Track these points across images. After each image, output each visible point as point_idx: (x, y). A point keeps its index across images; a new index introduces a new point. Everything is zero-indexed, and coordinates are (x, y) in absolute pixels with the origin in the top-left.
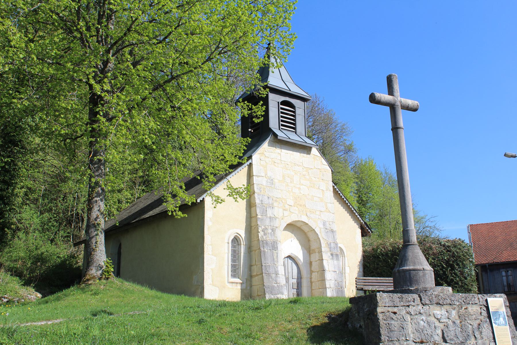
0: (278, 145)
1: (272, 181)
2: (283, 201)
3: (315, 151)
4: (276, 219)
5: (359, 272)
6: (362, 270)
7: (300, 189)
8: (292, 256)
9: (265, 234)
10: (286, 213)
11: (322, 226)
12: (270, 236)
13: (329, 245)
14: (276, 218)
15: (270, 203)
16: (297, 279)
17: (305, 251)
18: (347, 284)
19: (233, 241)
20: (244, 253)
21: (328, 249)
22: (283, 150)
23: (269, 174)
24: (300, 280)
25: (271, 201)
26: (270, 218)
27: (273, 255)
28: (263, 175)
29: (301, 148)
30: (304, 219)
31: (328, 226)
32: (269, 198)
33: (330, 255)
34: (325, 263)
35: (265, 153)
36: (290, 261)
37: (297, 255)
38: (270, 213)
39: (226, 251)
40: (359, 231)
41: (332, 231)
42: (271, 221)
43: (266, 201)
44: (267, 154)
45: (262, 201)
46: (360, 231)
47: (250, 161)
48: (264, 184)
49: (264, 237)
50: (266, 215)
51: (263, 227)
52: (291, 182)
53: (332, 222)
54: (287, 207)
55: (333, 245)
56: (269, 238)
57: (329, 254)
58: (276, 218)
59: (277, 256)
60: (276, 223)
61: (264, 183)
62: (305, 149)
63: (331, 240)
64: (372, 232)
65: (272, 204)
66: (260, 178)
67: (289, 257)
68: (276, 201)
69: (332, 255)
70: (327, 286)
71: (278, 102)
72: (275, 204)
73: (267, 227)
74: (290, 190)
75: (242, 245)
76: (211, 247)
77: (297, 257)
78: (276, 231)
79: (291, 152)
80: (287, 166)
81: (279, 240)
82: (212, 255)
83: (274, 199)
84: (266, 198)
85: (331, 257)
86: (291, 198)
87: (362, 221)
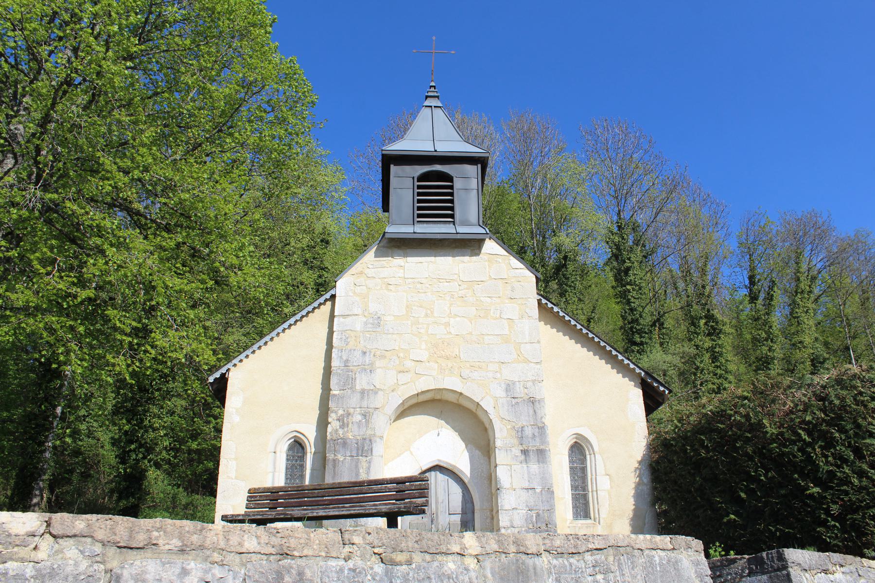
0: (400, 252)
1: (377, 321)
2: (401, 355)
3: (491, 246)
4: (376, 393)
5: (638, 485)
6: (646, 480)
7: (447, 324)
8: (442, 464)
10: (403, 378)
11: (500, 393)
14: (375, 391)
16: (464, 512)
17: (477, 453)
19: (291, 448)
20: (312, 470)
21: (516, 441)
23: (373, 307)
24: (469, 515)
25: (367, 359)
26: (363, 392)
27: (357, 467)
29: (456, 247)
31: (520, 391)
32: (365, 353)
33: (519, 453)
34: (502, 473)
35: (367, 271)
36: (440, 476)
37: (453, 463)
38: (361, 382)
40: (636, 396)
41: (532, 401)
42: (362, 398)
43: (356, 359)
44: (370, 272)
45: (347, 361)
46: (640, 392)
48: (358, 329)
49: (341, 432)
50: (352, 388)
51: (341, 412)
52: (427, 315)
53: (534, 381)
54: (409, 364)
55: (528, 431)
56: (352, 434)
57: (517, 451)
58: (375, 391)
59: (369, 468)
60: (378, 400)
61: (359, 327)
62: (469, 245)
63: (525, 420)
64: (670, 391)
65: (372, 364)
66: (349, 319)
67: (437, 468)
68: (383, 357)
69: (525, 452)
70: (501, 524)
72: (378, 364)
73: (351, 411)
74: (423, 331)
78: (375, 416)
79: (432, 259)
80: (419, 286)
81: (378, 434)
82: (236, 478)
83: (378, 353)
84: (358, 354)
85: (523, 457)
86: (423, 346)
87: (638, 371)
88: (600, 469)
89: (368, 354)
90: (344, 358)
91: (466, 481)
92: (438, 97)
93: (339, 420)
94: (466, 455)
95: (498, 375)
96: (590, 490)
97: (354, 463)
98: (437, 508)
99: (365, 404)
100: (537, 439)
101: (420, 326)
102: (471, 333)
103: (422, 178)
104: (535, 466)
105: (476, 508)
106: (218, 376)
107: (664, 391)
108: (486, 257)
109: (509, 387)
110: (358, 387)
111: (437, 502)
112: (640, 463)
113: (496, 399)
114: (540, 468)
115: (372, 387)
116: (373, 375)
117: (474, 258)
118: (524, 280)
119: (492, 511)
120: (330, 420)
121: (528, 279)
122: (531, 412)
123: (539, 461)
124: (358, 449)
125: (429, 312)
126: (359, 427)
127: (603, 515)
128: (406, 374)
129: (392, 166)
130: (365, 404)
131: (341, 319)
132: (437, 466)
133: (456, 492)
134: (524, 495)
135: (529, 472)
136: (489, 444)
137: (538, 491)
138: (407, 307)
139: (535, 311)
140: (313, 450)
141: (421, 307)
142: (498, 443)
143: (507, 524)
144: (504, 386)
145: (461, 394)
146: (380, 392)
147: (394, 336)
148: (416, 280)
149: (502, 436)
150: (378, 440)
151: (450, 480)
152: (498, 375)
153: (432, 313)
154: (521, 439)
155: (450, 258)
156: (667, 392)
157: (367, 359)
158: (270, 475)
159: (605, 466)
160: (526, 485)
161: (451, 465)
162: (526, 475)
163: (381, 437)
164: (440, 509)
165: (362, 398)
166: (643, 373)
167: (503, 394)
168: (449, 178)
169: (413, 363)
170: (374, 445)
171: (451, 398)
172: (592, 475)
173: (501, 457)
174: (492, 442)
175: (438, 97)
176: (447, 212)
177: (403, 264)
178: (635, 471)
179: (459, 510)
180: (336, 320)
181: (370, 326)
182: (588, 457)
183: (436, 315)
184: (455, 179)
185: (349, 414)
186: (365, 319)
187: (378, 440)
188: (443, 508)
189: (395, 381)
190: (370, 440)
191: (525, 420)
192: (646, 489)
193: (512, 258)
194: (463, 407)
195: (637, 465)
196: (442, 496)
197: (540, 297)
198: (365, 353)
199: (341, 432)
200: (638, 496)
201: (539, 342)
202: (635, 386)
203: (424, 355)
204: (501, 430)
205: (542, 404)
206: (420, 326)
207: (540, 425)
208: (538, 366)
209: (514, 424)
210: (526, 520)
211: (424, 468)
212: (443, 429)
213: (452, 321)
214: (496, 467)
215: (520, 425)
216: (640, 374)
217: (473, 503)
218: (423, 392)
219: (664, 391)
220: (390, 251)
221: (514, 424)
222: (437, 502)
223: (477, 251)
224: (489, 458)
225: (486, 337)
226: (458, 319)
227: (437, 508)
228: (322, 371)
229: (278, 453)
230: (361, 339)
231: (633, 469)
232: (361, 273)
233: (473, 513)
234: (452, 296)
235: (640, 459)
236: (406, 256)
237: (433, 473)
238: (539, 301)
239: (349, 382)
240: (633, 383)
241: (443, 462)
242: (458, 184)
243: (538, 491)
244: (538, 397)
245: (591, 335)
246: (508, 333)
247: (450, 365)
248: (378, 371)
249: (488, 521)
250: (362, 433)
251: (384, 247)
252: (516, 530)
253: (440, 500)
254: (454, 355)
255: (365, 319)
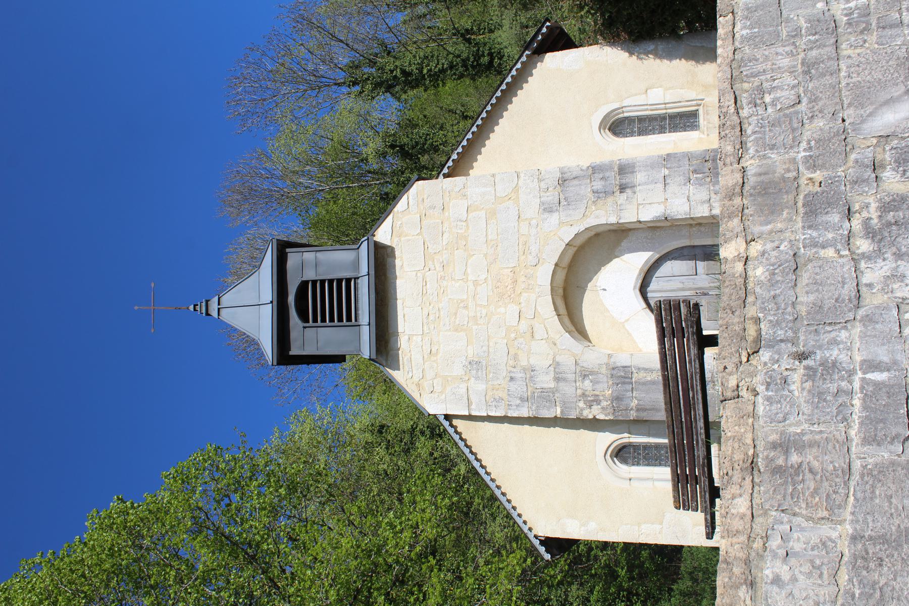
0: (392, 340)
1: (475, 365)
2: (513, 335)
3: (383, 234)
4: (558, 364)
5: (658, 56)
7: (476, 283)
9: (598, 402)
10: (540, 333)
11: (554, 218)
12: (599, 387)
13: (601, 195)
14: (556, 364)
15: (522, 375)
16: (694, 258)
17: (624, 244)
18: (694, 96)
19: (624, 461)
20: (649, 435)
21: (610, 200)
22: (400, 329)
23: (458, 370)
24: (698, 251)
26: (557, 379)
27: (644, 384)
28: (463, 386)
29: (385, 275)
30: (544, 275)
31: (551, 196)
32: (512, 379)
33: (624, 196)
34: (648, 214)
35: (416, 379)
36: (653, 286)
38: (546, 381)
39: (649, 484)
40: (553, 60)
41: (563, 181)
42: (565, 380)
43: (518, 388)
44: (417, 375)
45: (521, 399)
46: (549, 56)
47: (441, 418)
48: (484, 386)
49: (604, 404)
50: (554, 391)
51: (581, 404)
52: (466, 307)
53: (540, 180)
54: (524, 326)
55: (598, 185)
56: (606, 390)
57: (622, 198)
58: (556, 364)
59: (645, 370)
60: (567, 361)
61: (481, 387)
62: (382, 259)
63: (585, 190)
64: (547, 20)
65: (524, 370)
66: (472, 397)
67: (643, 290)
68: (516, 357)
69: (623, 188)
71: (304, 327)
72: (524, 363)
73: (579, 392)
74: (484, 312)
75: (632, 440)
76: (643, 526)
77: (641, 270)
78: (585, 365)
79: (399, 302)
80: (431, 317)
81: (605, 360)
82: (661, 523)
83: (511, 363)
84: (513, 386)
86: (502, 310)
87: (524, 59)
88: (640, 100)
89: (513, 375)
90: (518, 402)
91: (657, 256)
92: (207, 301)
93: (590, 407)
94: (628, 257)
95: (534, 222)
96: (664, 111)
97: (640, 387)
98: (690, 289)
99: (571, 377)
100: (607, 174)
101: (479, 314)
102: (485, 255)
103: (304, 317)
104: (639, 176)
105: (688, 244)
106: (544, 549)
107: (547, 27)
108: (396, 240)
109: (548, 209)
110: (552, 385)
111: (683, 290)
112: (631, 54)
113: (561, 223)
114: (640, 171)
115: (552, 368)
116: (537, 368)
117: (397, 253)
118: (421, 195)
119: (691, 225)
120: (591, 417)
121: (419, 189)
122: (576, 182)
123: (633, 172)
124: (624, 383)
125: (462, 305)
126: (598, 382)
127: (693, 95)
128: (535, 330)
129: (291, 353)
130: (571, 377)
131: (473, 407)
132: (641, 290)
133: (669, 267)
134: (672, 188)
135: (646, 183)
136: (614, 231)
137: (667, 172)
138: (456, 330)
139: (458, 180)
140: (626, 435)
141: (456, 314)
142: (613, 220)
143: (706, 206)
144: (546, 215)
145: (556, 265)
146: (558, 359)
147: (491, 344)
148: (425, 321)
149: (604, 215)
150: (612, 360)
151: (656, 275)
152: (534, 222)
153: (462, 301)
154: (607, 193)
155: (398, 282)
156: (548, 24)
157: (519, 375)
158: (656, 483)
159: (636, 95)
160: (661, 186)
161: (640, 274)
162: (649, 187)
163: (610, 356)
164: (691, 285)
165: (565, 380)
166: (527, 52)
167: (555, 216)
168: (303, 286)
169: (522, 321)
170: (619, 364)
171: (561, 275)
172: (647, 110)
173: (629, 216)
174: (612, 228)
175: (207, 301)
176: (343, 288)
177: (407, 337)
178: (641, 59)
179: (692, 263)
180: (474, 413)
181: (480, 373)
182: (626, 115)
183: (465, 297)
184: (305, 279)
185: (584, 395)
186: (473, 380)
187: (612, 360)
188: (689, 283)
189: (544, 341)
190: (613, 369)
191: (585, 190)
192: (661, 45)
193: (395, 209)
194: (571, 262)
195: (634, 57)
196: (675, 284)
197: (441, 176)
198: (512, 379)
199: (604, 404)
200: (670, 55)
201: (493, 175)
202: (542, 61)
203: (513, 309)
204: (597, 217)
205: (566, 170)
206: (479, 314)
207: (590, 171)
208: (522, 175)
209: (590, 202)
210: (701, 185)
211: (644, 306)
212: (598, 284)
213: (471, 278)
214: (640, 222)
215: (590, 195)
216: (527, 56)
217: (683, 248)
218: (556, 309)
219: (547, 27)
220: (391, 352)
221: (590, 202)
222: (683, 290)
223: (389, 250)
224: (630, 230)
225: (490, 238)
226: (469, 270)
227: (690, 289)
228: (534, 427)
229: (631, 476)
230: (496, 383)
231: (639, 62)
232: (418, 385)
233: (694, 247)
234: (443, 278)
235: (627, 54)
236: (396, 334)
237: (649, 295)
238: (446, 176)
239: (547, 396)
240: (539, 64)
241: (636, 283)
242: (310, 275)
243: (667, 172)
244: (558, 175)
245: (484, 115)
246: (483, 212)
247: (523, 279)
248: (532, 361)
249: (703, 229)
250: (605, 379)
251: (387, 360)
252: (713, 196)
253: (681, 286)
254: (512, 274)
255: (473, 380)
